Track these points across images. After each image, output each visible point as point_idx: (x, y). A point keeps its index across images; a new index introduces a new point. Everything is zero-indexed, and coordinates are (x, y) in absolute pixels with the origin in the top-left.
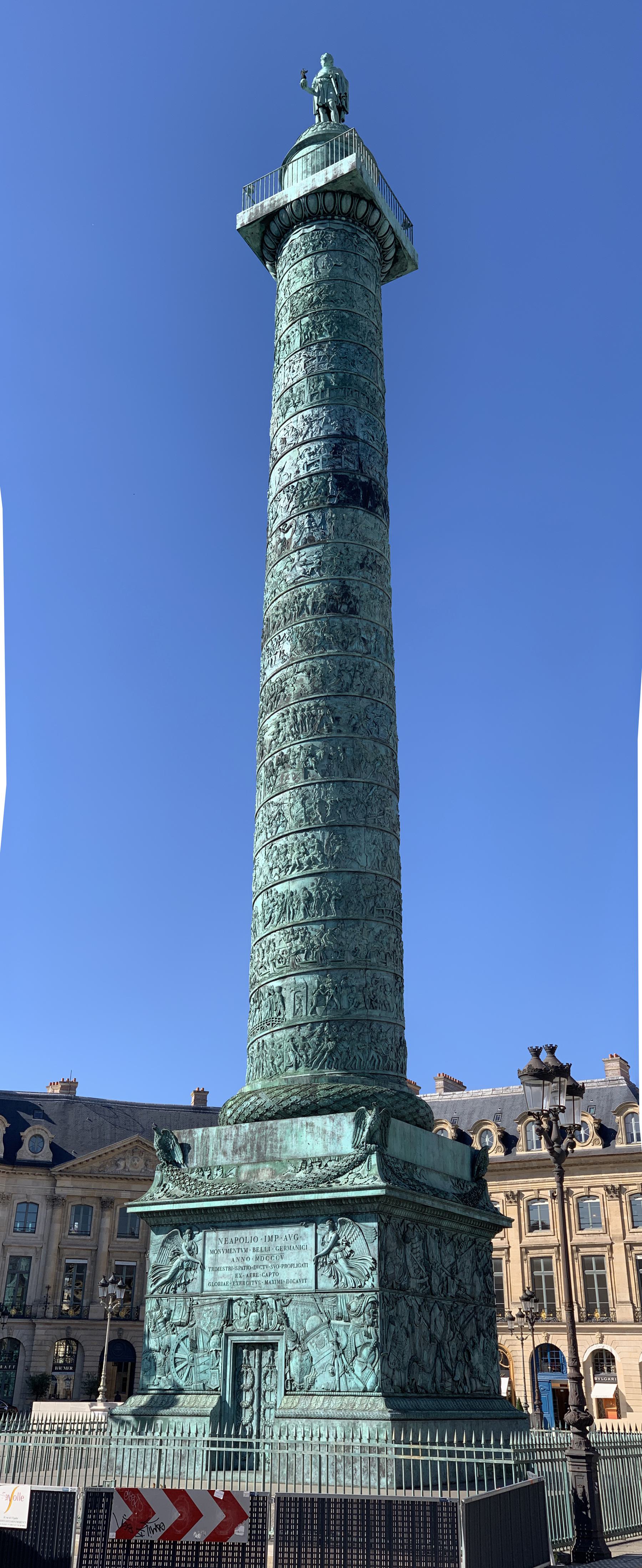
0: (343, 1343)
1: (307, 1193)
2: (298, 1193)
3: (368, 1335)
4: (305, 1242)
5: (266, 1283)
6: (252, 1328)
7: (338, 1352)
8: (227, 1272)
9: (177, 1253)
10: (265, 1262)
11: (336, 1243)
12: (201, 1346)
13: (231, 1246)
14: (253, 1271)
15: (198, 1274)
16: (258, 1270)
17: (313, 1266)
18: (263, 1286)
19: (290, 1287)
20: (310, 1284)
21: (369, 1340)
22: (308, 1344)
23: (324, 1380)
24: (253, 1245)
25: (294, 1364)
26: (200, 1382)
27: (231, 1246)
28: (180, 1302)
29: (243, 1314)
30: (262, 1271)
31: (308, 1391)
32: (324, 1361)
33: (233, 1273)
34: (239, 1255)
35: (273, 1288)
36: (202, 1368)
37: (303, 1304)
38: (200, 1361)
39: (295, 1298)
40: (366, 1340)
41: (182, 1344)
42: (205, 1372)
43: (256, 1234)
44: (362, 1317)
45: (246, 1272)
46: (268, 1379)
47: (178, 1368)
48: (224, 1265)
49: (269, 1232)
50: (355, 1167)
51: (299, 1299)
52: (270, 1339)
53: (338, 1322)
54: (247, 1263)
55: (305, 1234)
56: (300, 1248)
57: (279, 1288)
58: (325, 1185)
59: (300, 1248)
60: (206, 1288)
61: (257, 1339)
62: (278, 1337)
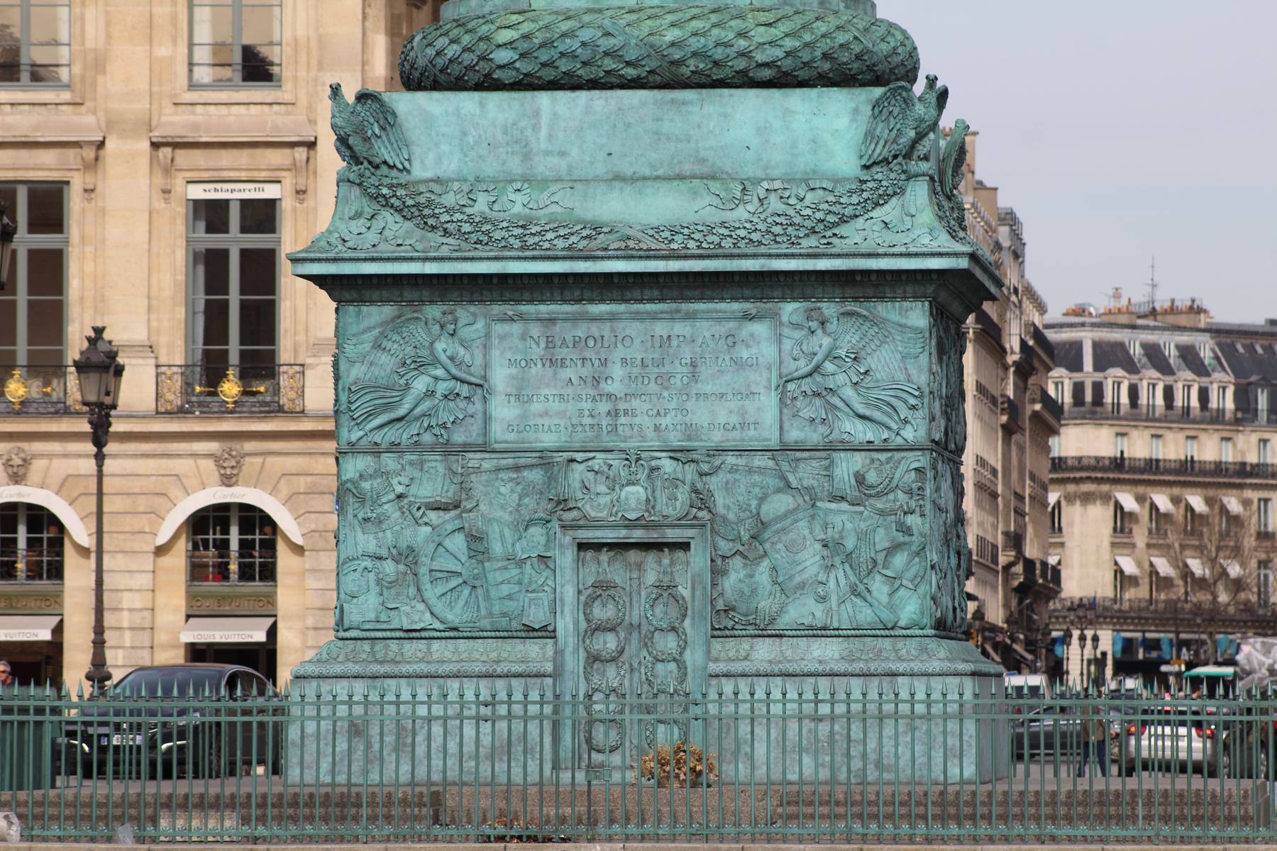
0: (850, 543)
1: (778, 256)
2: (755, 256)
3: (907, 531)
4: (754, 350)
5: (657, 428)
6: (632, 516)
7: (837, 560)
8: (555, 406)
9: (420, 366)
10: (653, 387)
11: (831, 356)
12: (497, 548)
13: (562, 353)
14: (622, 406)
15: (478, 406)
16: (636, 403)
17: (774, 398)
18: (650, 434)
19: (717, 438)
20: (766, 434)
21: (907, 539)
22: (767, 546)
23: (802, 610)
24: (620, 352)
25: (732, 581)
26: (504, 615)
28: (436, 464)
29: (602, 488)
30: (646, 406)
31: (766, 630)
32: (805, 576)
33: (571, 408)
34: (586, 371)
35: (675, 440)
36: (505, 590)
37: (750, 471)
38: (499, 577)
39: (731, 459)
40: (901, 538)
41: (447, 543)
42: (510, 597)
43: (628, 332)
44: (891, 496)
45: (603, 407)
46: (659, 609)
47: (440, 589)
48: (547, 391)
49: (660, 329)
50: (877, 204)
51: (741, 461)
52: (672, 535)
53: (833, 506)
54: (608, 387)
55: (752, 335)
56: (739, 364)
57: (689, 438)
58: (812, 241)
59: (739, 364)
60: (498, 432)
61: (638, 535)
62: (690, 533)
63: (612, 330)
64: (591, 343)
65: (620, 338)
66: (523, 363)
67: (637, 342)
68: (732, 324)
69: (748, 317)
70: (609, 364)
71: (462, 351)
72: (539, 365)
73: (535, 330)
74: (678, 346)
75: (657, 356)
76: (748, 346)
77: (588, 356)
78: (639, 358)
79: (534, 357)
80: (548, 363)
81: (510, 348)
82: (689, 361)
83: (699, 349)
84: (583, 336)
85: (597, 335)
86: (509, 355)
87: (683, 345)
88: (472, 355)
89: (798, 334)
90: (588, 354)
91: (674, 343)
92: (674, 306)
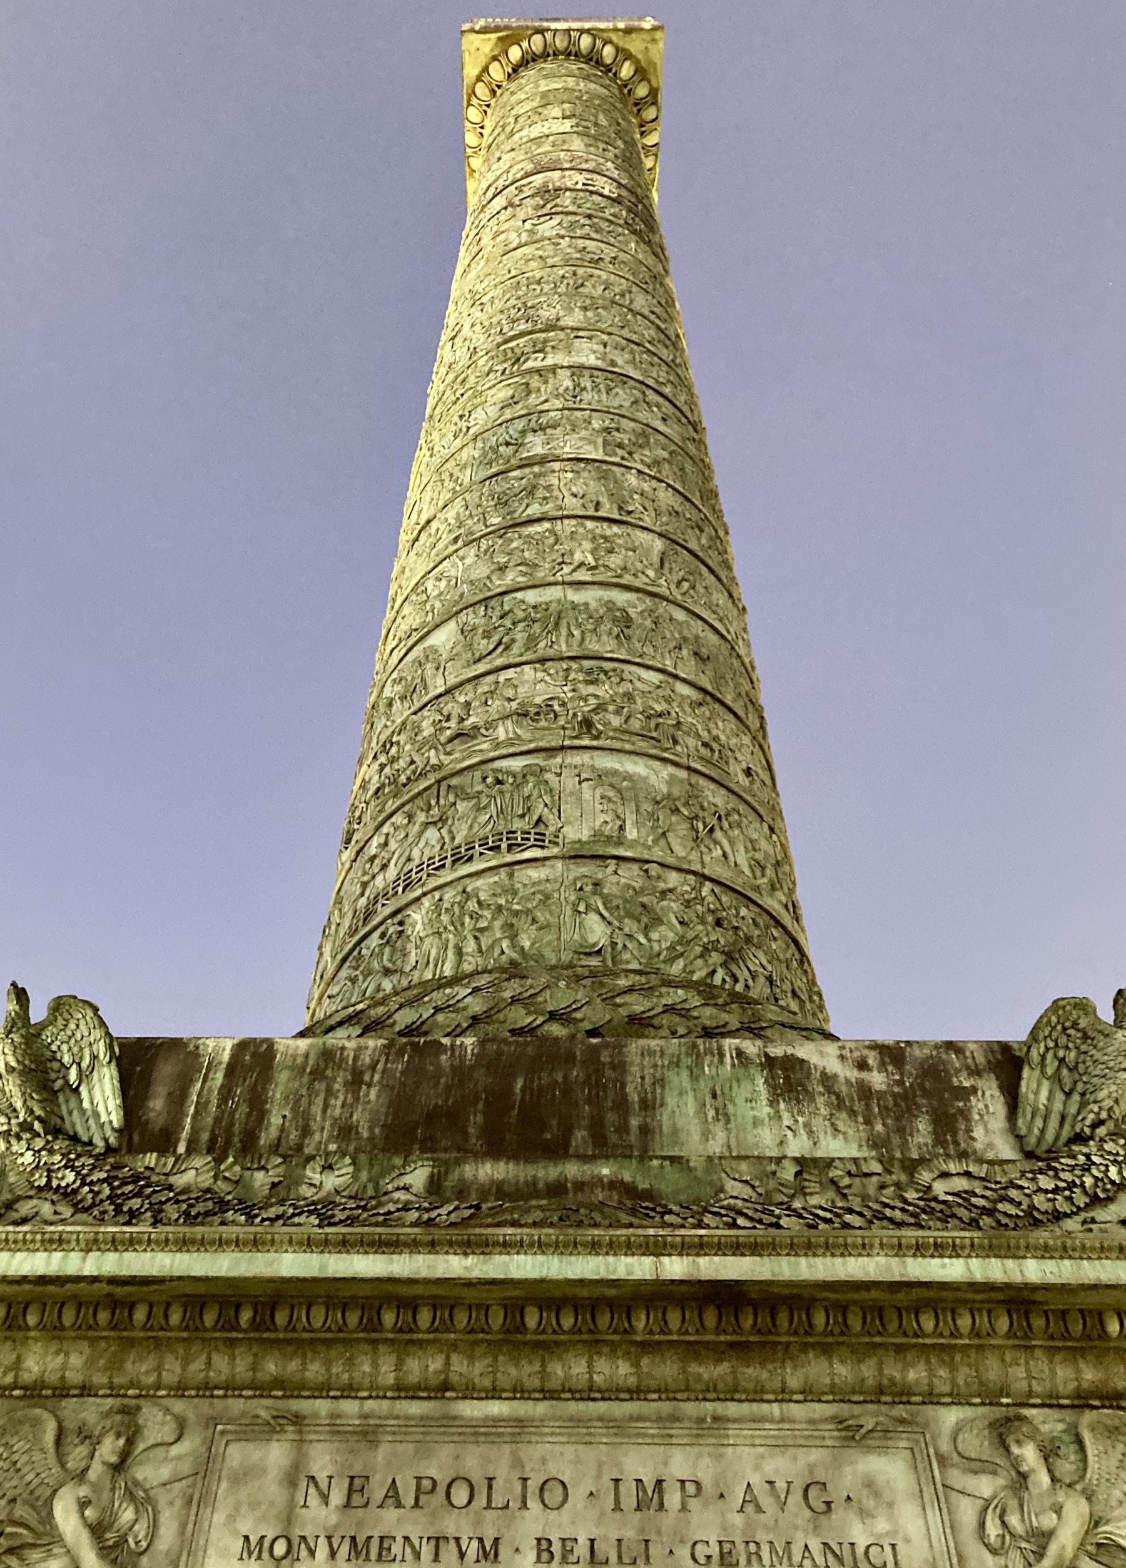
4: (882, 1525)
27: (389, 1520)
43: (553, 1469)
49: (638, 1464)
55: (869, 1484)
63: (517, 1463)
64: (460, 1495)
65: (533, 1485)
66: (280, 1548)
67: (578, 1495)
68: (815, 1455)
69: (852, 1436)
70: (504, 1552)
71: (128, 1515)
72: (322, 1552)
73: (323, 1461)
74: (684, 1508)
75: (630, 1534)
76: (864, 1514)
77: (451, 1532)
78: (583, 1540)
79: (308, 1532)
80: (345, 1548)
81: (254, 1505)
82: (714, 1550)
83: (738, 1519)
84: (443, 1480)
85: (477, 1477)
86: (245, 1526)
87: (693, 1504)
88: (154, 1526)
89: (986, 1485)
90: (453, 1524)
91: (673, 1499)
92: (666, 1407)
